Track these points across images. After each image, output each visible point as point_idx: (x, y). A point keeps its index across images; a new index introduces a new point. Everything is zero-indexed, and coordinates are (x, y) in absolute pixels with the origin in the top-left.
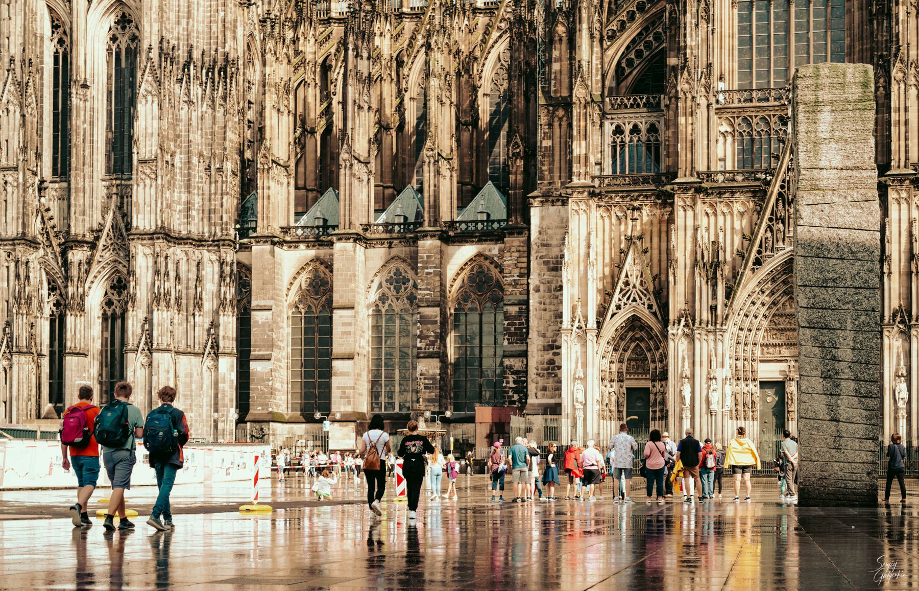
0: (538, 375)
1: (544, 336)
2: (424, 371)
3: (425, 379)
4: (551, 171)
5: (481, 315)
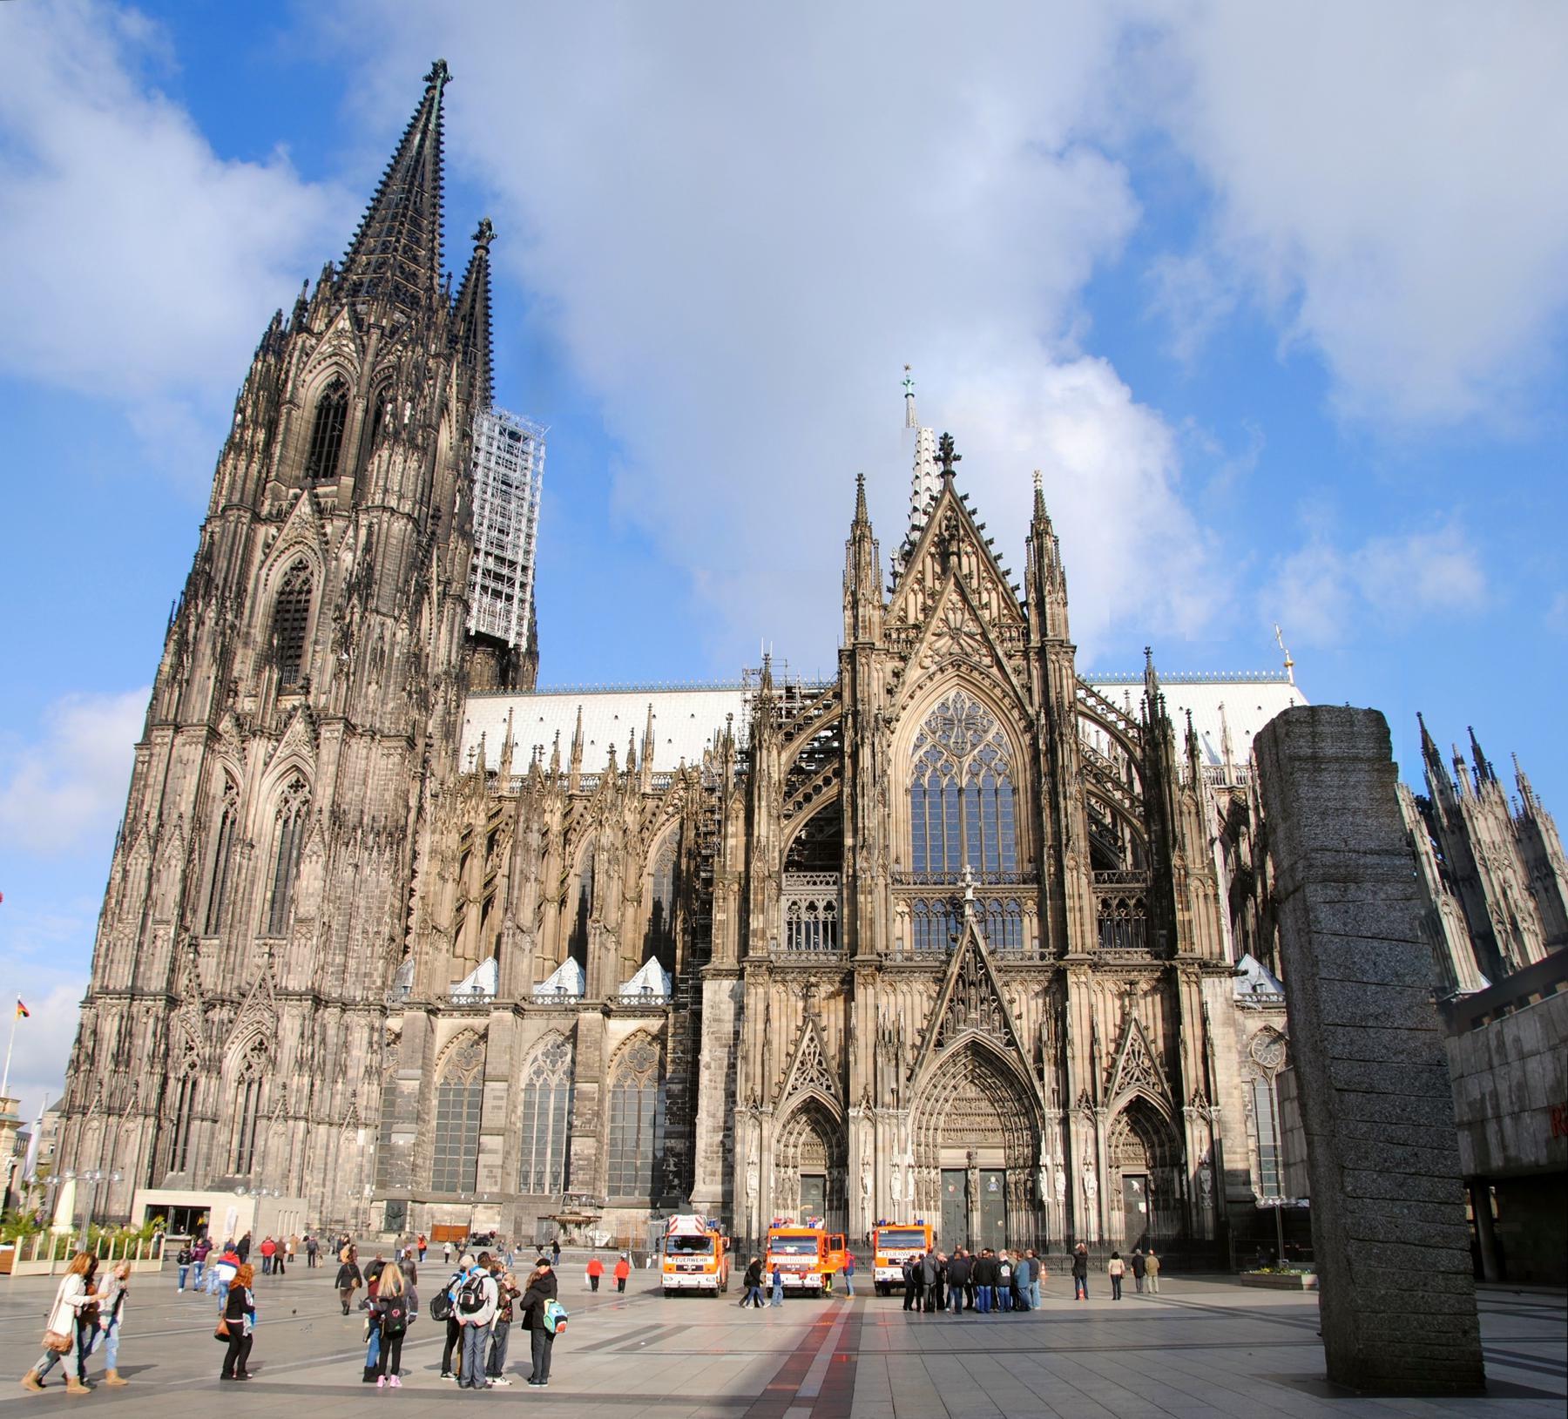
1: (714, 1116)
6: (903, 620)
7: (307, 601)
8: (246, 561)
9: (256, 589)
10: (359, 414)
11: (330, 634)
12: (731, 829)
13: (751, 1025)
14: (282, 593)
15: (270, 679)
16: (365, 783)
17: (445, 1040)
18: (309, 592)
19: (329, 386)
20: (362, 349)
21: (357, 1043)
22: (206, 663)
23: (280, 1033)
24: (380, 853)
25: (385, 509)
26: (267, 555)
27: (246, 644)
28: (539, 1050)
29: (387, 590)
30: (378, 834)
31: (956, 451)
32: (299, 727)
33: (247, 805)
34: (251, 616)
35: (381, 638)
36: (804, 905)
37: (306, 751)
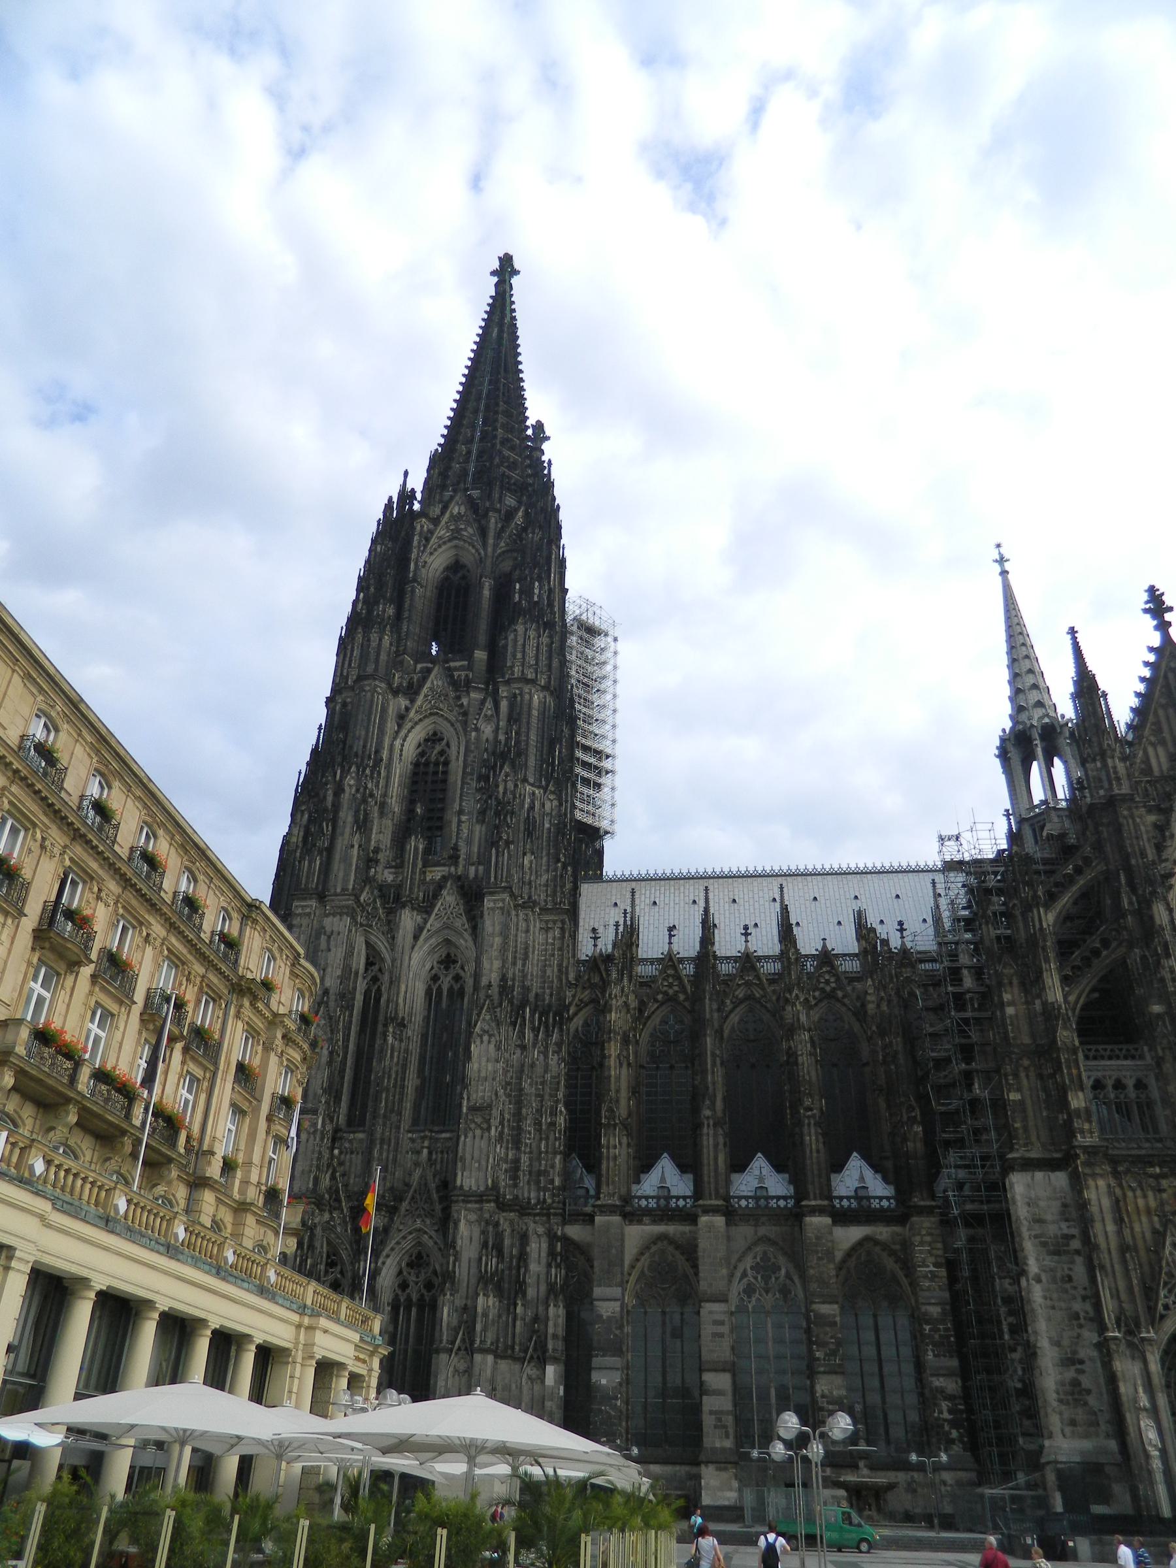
0: (1061, 1401)
2: (826, 1392)
3: (828, 1403)
4: (1026, 1129)
5: (875, 1316)
6: (1148, 771)
7: (445, 773)
8: (382, 731)
10: (486, 593)
11: (471, 804)
12: (1007, 997)
13: (1098, 1226)
14: (416, 765)
15: (416, 848)
16: (526, 958)
17: (635, 1251)
18: (446, 763)
19: (447, 569)
20: (483, 532)
22: (348, 830)
23: (459, 1242)
25: (525, 680)
26: (400, 726)
28: (748, 1262)
29: (532, 762)
30: (544, 1013)
31: (1168, 600)
32: (449, 898)
33: (394, 982)
35: (532, 808)
36: (1110, 1083)
37: (461, 922)
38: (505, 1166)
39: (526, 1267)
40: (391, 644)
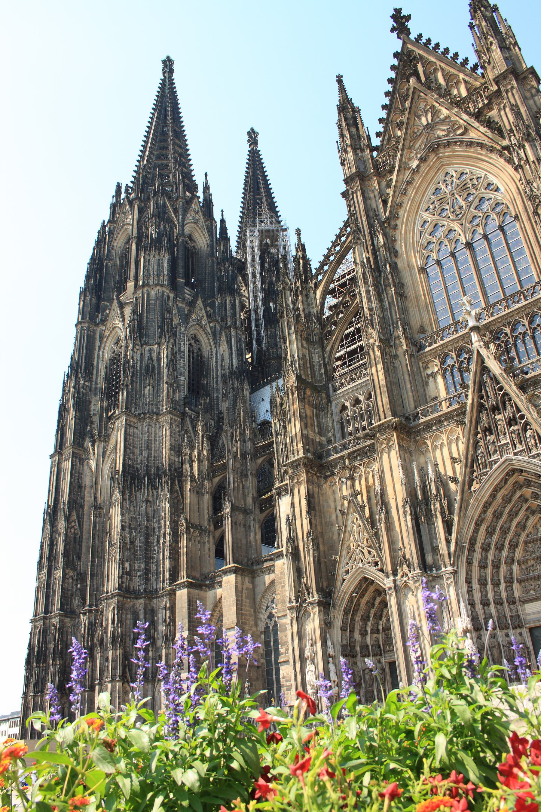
9: (98, 362)
21: (160, 621)
24: (162, 490)
26: (101, 341)
27: (95, 395)
34: (97, 378)
35: (151, 358)
38: (139, 574)
39: (156, 630)
40: (91, 300)
